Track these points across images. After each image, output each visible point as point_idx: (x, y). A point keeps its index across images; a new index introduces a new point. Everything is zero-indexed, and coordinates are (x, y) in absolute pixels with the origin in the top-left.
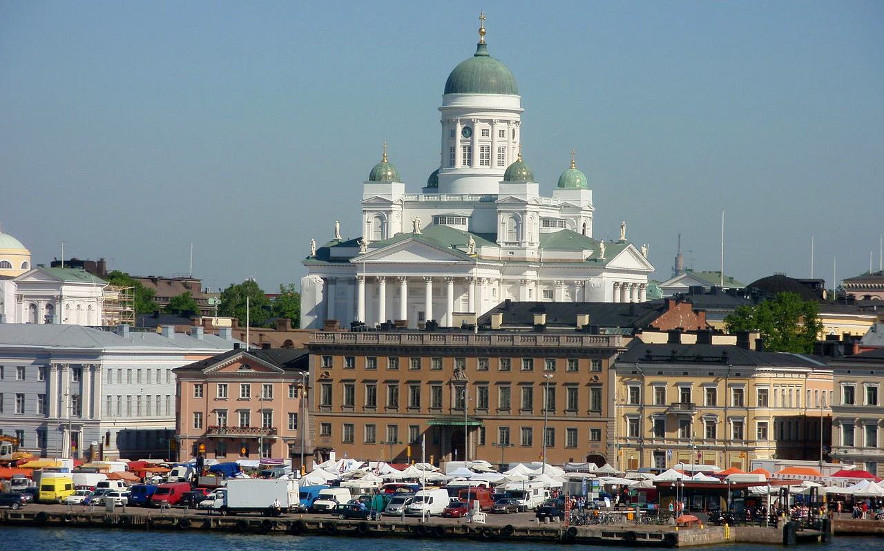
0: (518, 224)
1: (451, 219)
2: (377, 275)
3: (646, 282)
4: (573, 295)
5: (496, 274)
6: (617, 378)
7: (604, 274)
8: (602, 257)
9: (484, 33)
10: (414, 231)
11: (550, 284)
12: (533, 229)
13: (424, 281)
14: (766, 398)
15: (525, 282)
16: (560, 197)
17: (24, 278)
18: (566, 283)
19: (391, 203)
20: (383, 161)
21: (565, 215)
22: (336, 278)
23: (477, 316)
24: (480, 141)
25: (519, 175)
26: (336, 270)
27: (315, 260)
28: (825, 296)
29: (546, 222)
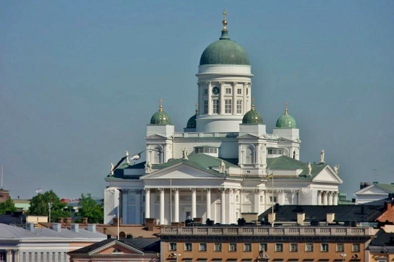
1: (207, 149)
2: (158, 187)
3: (337, 190)
4: (290, 200)
5: (238, 186)
6: (370, 256)
7: (312, 185)
8: (310, 174)
9: (226, 24)
10: (184, 157)
11: (275, 192)
12: (262, 156)
13: (190, 191)
15: (258, 191)
16: (278, 134)
18: (285, 191)
19: (166, 139)
20: (160, 110)
21: (281, 146)
22: (128, 190)
23: (259, 214)
24: (224, 96)
26: (130, 185)
27: (113, 178)
29: (270, 151)
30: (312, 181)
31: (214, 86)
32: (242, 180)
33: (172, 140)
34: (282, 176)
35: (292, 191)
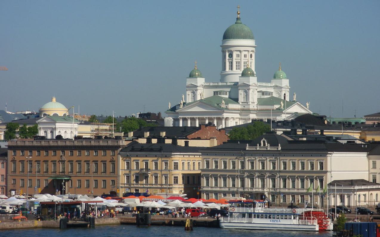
1: (220, 93)
2: (187, 117)
6: (121, 158)
7: (283, 115)
9: (239, 14)
14: (177, 166)
17: (42, 120)
19: (197, 86)
20: (195, 69)
24: (235, 59)
25: (247, 74)
27: (170, 111)
28: (326, 122)
30: (282, 113)
31: (229, 53)
33: (203, 87)
34: (266, 109)
35: (263, 119)
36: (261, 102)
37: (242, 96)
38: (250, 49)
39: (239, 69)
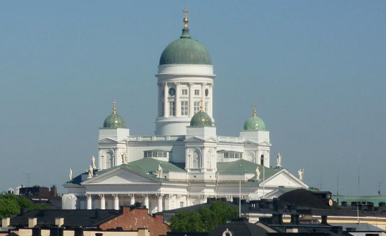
0: (112, 157)
1: (155, 153)
2: (99, 193)
7: (259, 191)
9: (187, 22)
19: (116, 143)
20: (113, 113)
24: (180, 98)
25: (200, 122)
27: (71, 184)
28: (331, 203)
30: (258, 186)
32: (187, 185)
33: (126, 144)
34: (230, 181)
35: (227, 197)
36: (223, 168)
37: (192, 158)
38: (205, 81)
39: (186, 113)
